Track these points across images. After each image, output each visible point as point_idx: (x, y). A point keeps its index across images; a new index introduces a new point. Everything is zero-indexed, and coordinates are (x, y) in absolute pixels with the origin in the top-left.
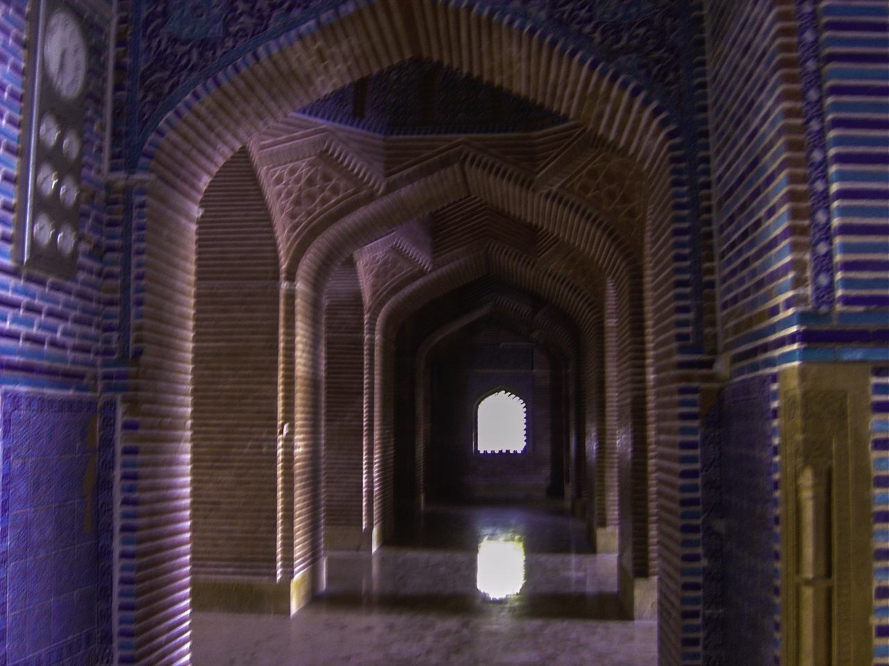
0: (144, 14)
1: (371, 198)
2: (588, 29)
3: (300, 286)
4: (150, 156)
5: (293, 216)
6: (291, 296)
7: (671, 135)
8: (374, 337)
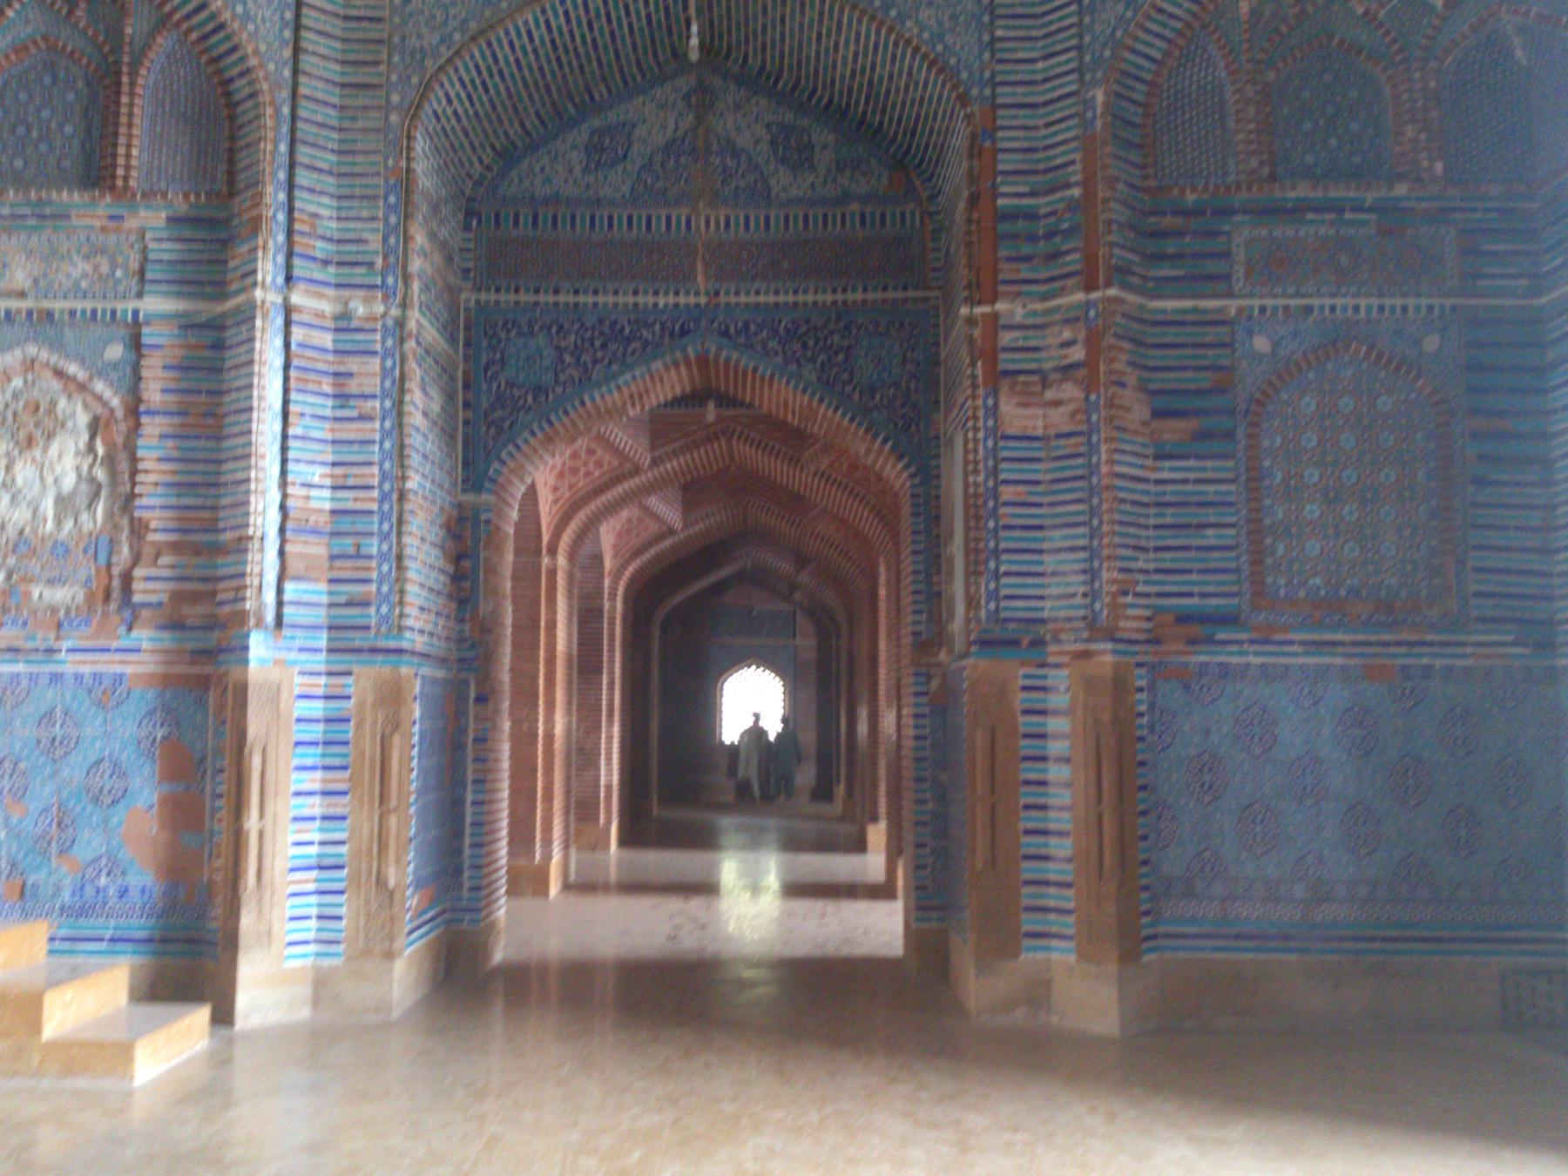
0: (484, 360)
1: (636, 471)
2: (849, 389)
3: (562, 561)
4: (493, 481)
5: (555, 489)
6: (552, 573)
7: (912, 476)
8: (615, 607)
